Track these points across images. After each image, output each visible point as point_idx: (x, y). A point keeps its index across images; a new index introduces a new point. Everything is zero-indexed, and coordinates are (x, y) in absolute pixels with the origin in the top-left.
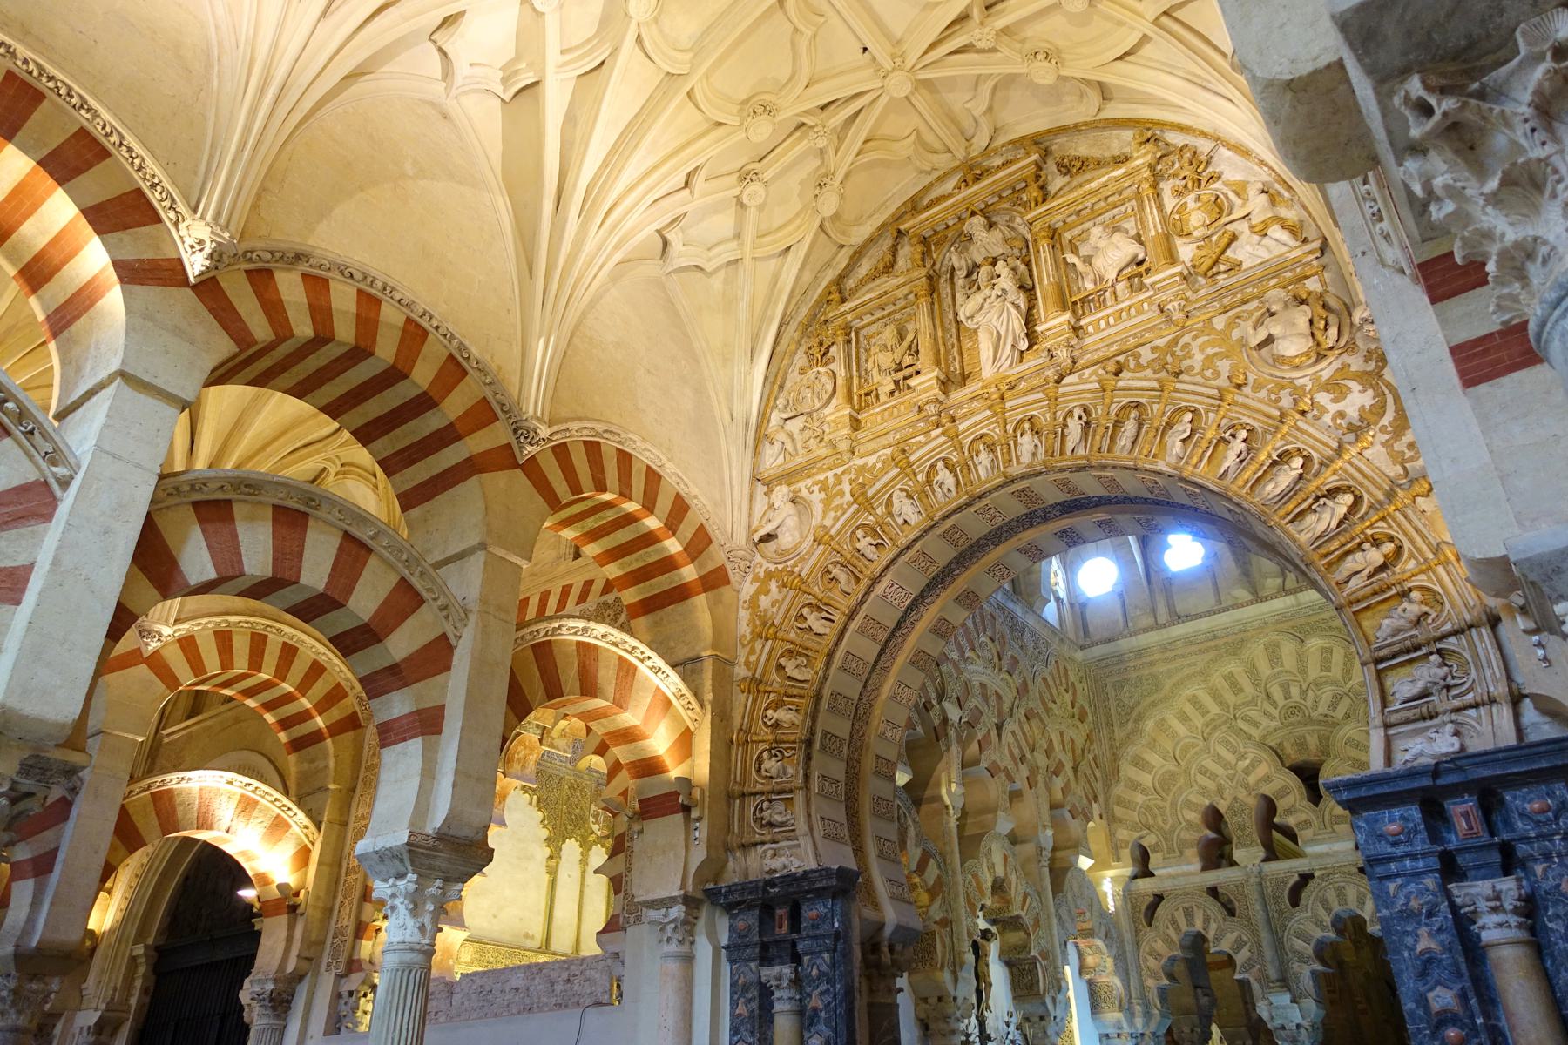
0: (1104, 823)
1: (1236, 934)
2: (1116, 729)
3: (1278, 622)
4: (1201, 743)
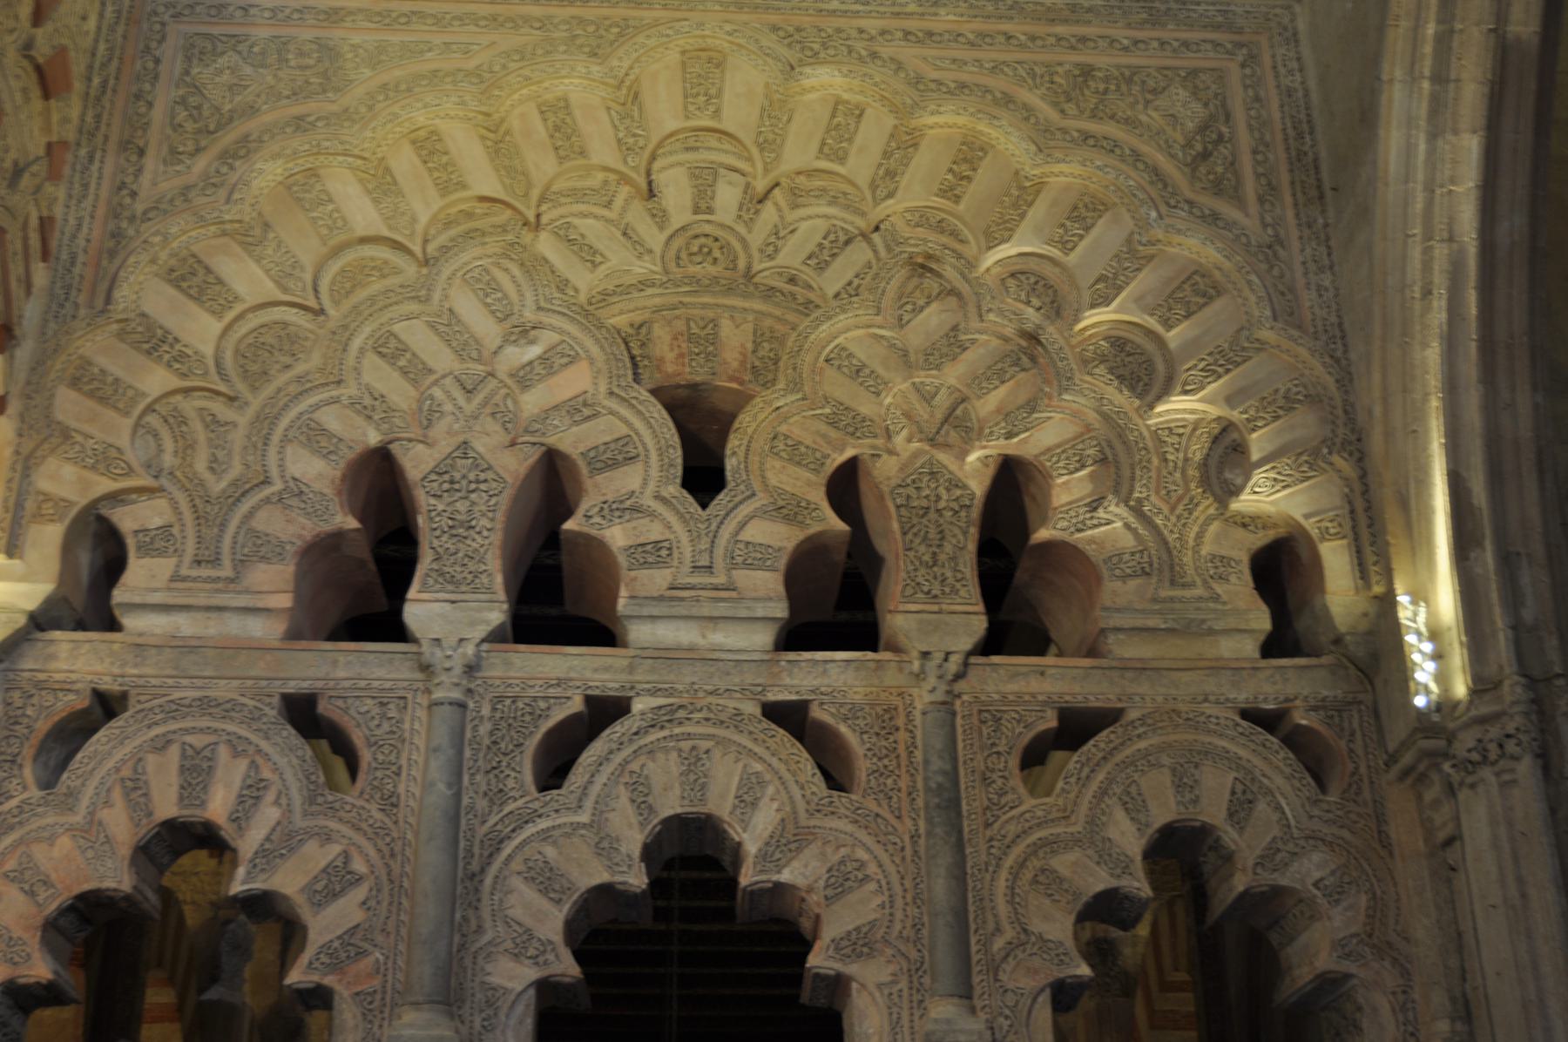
1: (336, 849)
2: (150, 163)
4: (410, 270)
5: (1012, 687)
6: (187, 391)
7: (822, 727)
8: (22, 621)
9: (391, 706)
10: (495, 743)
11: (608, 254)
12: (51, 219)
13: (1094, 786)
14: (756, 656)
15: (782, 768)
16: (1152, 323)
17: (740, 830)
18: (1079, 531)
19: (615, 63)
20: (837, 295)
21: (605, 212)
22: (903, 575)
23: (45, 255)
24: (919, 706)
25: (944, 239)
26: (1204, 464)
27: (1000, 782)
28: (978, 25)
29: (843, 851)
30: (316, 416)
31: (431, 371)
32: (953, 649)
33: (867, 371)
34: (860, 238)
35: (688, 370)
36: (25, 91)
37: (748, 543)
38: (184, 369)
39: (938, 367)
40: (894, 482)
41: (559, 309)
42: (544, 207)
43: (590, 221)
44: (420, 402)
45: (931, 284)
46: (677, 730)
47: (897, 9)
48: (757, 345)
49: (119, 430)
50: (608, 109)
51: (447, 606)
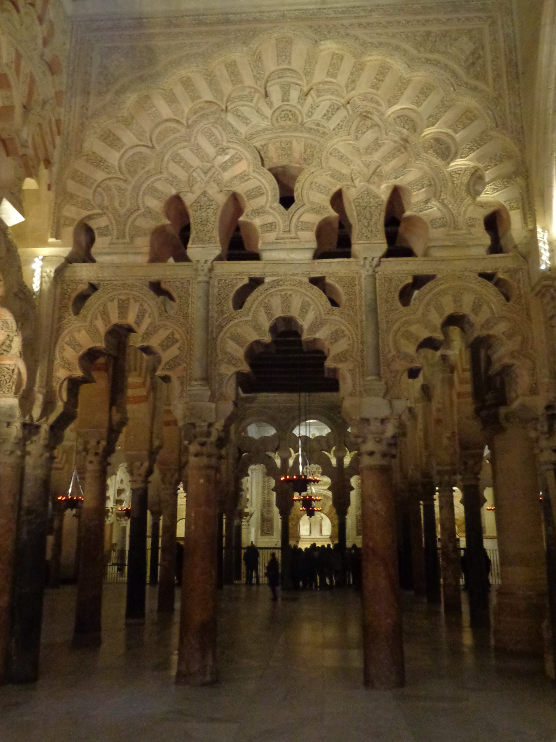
0: (51, 195)
1: (169, 332)
3: (297, 18)
4: (183, 130)
5: (396, 268)
6: (110, 179)
7: (330, 285)
8: (63, 260)
9: (185, 284)
10: (219, 295)
11: (252, 120)
12: (60, 120)
13: (424, 302)
14: (307, 262)
15: (316, 300)
16: (450, 131)
17: (302, 321)
18: (421, 211)
19: (251, 45)
20: (334, 129)
21: (250, 104)
22: (357, 230)
23: (59, 133)
24: (363, 276)
25: (374, 105)
26: (468, 184)
27: (392, 301)
28: (388, 19)
29: (336, 327)
30: (154, 185)
31: (192, 167)
32: (375, 256)
33: (345, 157)
34: (342, 107)
35: (281, 161)
36: (44, 72)
37: (302, 222)
38: (108, 171)
39: (370, 154)
40: (354, 197)
41: (235, 141)
42: (229, 104)
43: (245, 108)
44: (189, 178)
45: (369, 123)
46: (280, 288)
47: (356, 15)
48: (306, 150)
49: (89, 194)
50: (250, 64)
51: (201, 249)
